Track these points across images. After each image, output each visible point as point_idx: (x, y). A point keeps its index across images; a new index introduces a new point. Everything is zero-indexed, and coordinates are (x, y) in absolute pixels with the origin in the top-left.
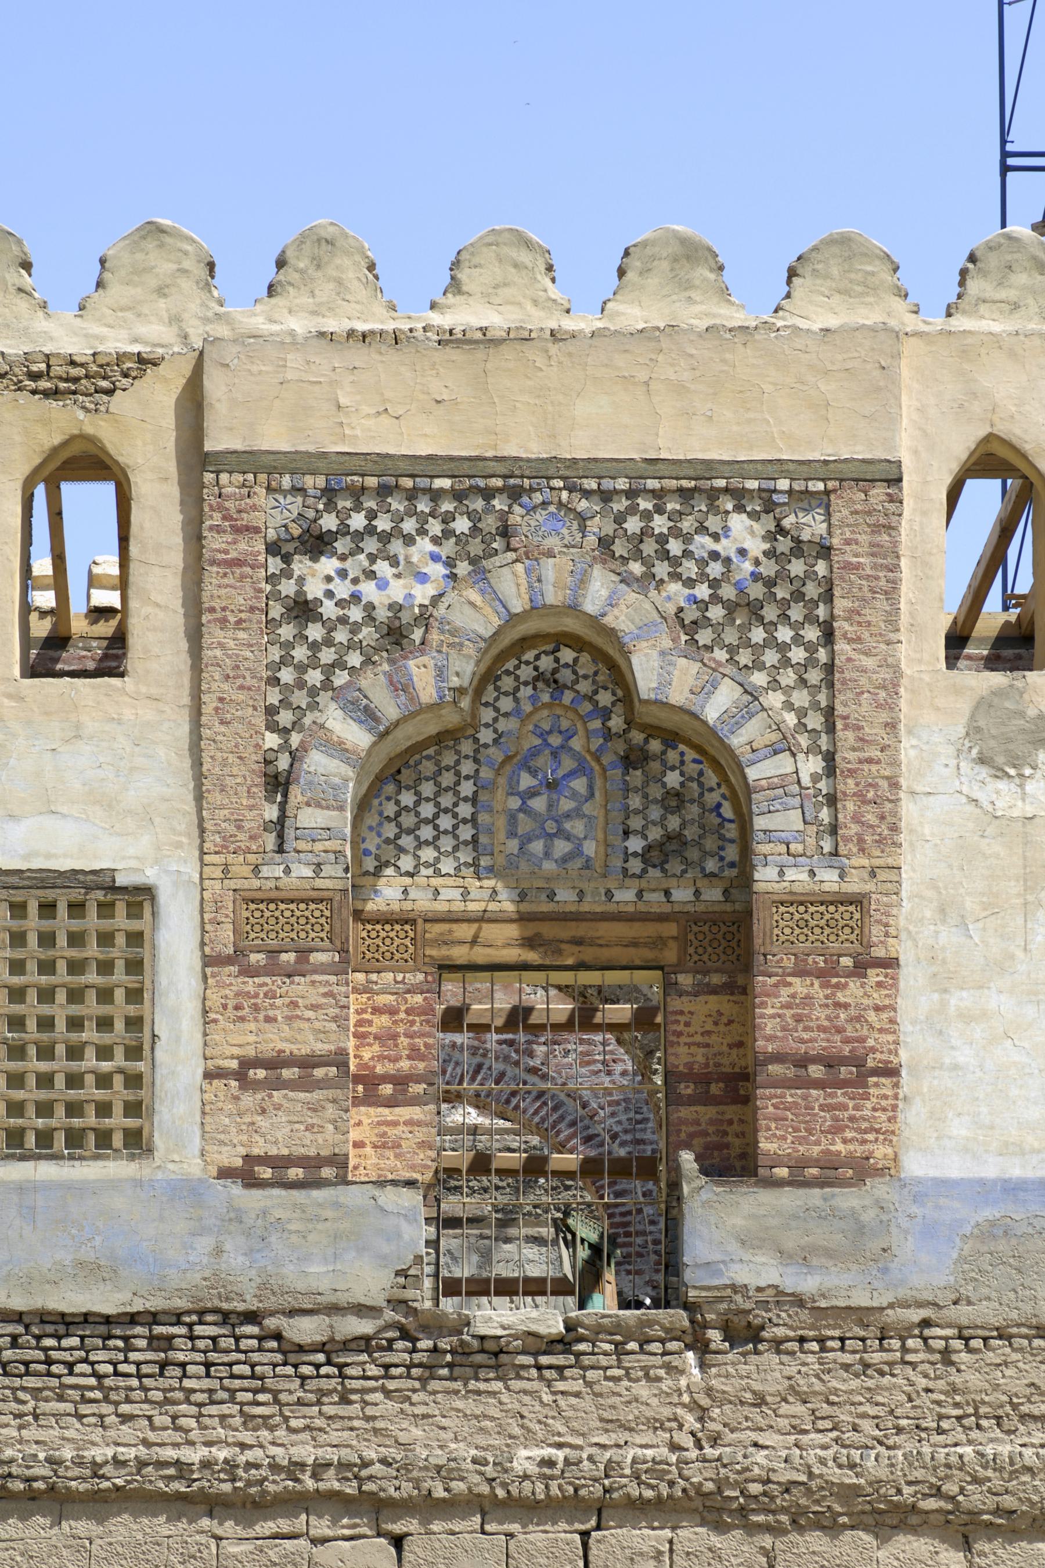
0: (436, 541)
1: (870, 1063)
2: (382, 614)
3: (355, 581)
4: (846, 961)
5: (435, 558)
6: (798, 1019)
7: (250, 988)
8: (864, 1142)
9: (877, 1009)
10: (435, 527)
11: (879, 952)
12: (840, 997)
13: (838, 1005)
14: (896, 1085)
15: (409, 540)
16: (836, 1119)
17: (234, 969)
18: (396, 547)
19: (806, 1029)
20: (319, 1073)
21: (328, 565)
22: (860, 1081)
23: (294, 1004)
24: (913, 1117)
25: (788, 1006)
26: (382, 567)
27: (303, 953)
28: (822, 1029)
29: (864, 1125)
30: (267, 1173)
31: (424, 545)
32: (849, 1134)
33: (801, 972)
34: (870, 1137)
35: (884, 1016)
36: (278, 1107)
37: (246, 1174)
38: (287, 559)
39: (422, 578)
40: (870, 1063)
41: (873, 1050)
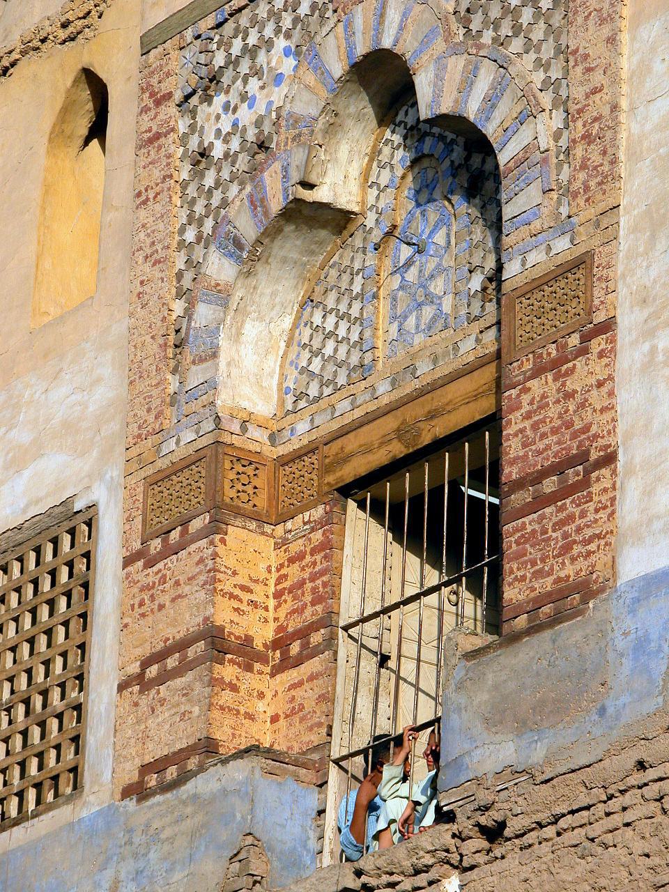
0: (288, 36)
1: (594, 455)
2: (251, 135)
3: (235, 110)
4: (574, 340)
5: (287, 52)
6: (535, 427)
7: (150, 580)
8: (589, 553)
9: (600, 384)
10: (287, 22)
11: (600, 317)
12: (571, 384)
13: (569, 395)
14: (614, 472)
15: (269, 44)
16: (566, 536)
17: (140, 564)
18: (262, 58)
19: (544, 436)
20: (191, 652)
21: (219, 100)
22: (585, 483)
23: (177, 583)
24: (630, 507)
25: (528, 416)
26: (254, 84)
27: (185, 524)
28: (555, 431)
29: (588, 533)
30: (152, 780)
31: (281, 43)
32: (576, 549)
33: (537, 372)
34: (592, 547)
35: (604, 390)
36: (162, 702)
37: (137, 791)
38: (193, 113)
39: (278, 79)
40: (594, 455)
41: (596, 436)
